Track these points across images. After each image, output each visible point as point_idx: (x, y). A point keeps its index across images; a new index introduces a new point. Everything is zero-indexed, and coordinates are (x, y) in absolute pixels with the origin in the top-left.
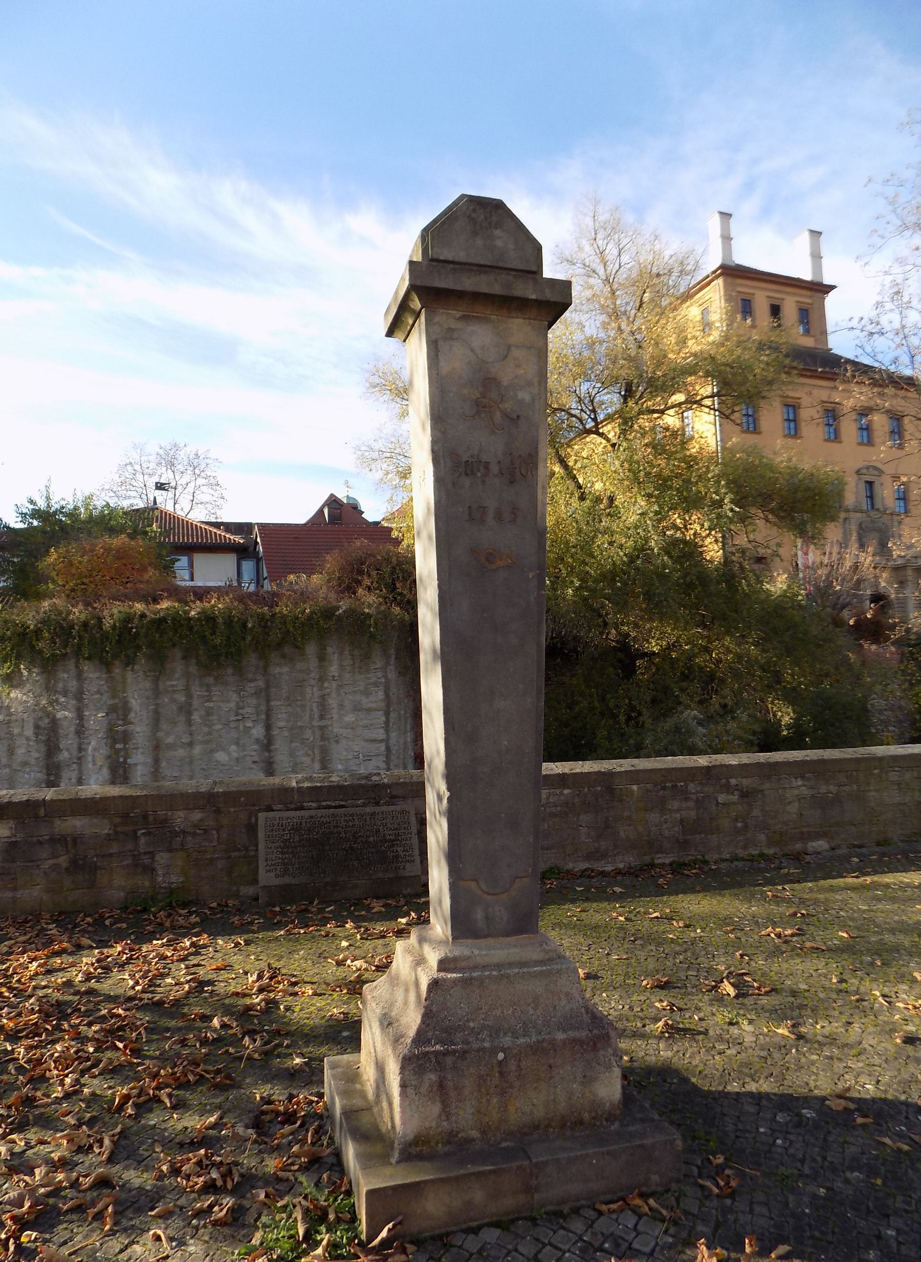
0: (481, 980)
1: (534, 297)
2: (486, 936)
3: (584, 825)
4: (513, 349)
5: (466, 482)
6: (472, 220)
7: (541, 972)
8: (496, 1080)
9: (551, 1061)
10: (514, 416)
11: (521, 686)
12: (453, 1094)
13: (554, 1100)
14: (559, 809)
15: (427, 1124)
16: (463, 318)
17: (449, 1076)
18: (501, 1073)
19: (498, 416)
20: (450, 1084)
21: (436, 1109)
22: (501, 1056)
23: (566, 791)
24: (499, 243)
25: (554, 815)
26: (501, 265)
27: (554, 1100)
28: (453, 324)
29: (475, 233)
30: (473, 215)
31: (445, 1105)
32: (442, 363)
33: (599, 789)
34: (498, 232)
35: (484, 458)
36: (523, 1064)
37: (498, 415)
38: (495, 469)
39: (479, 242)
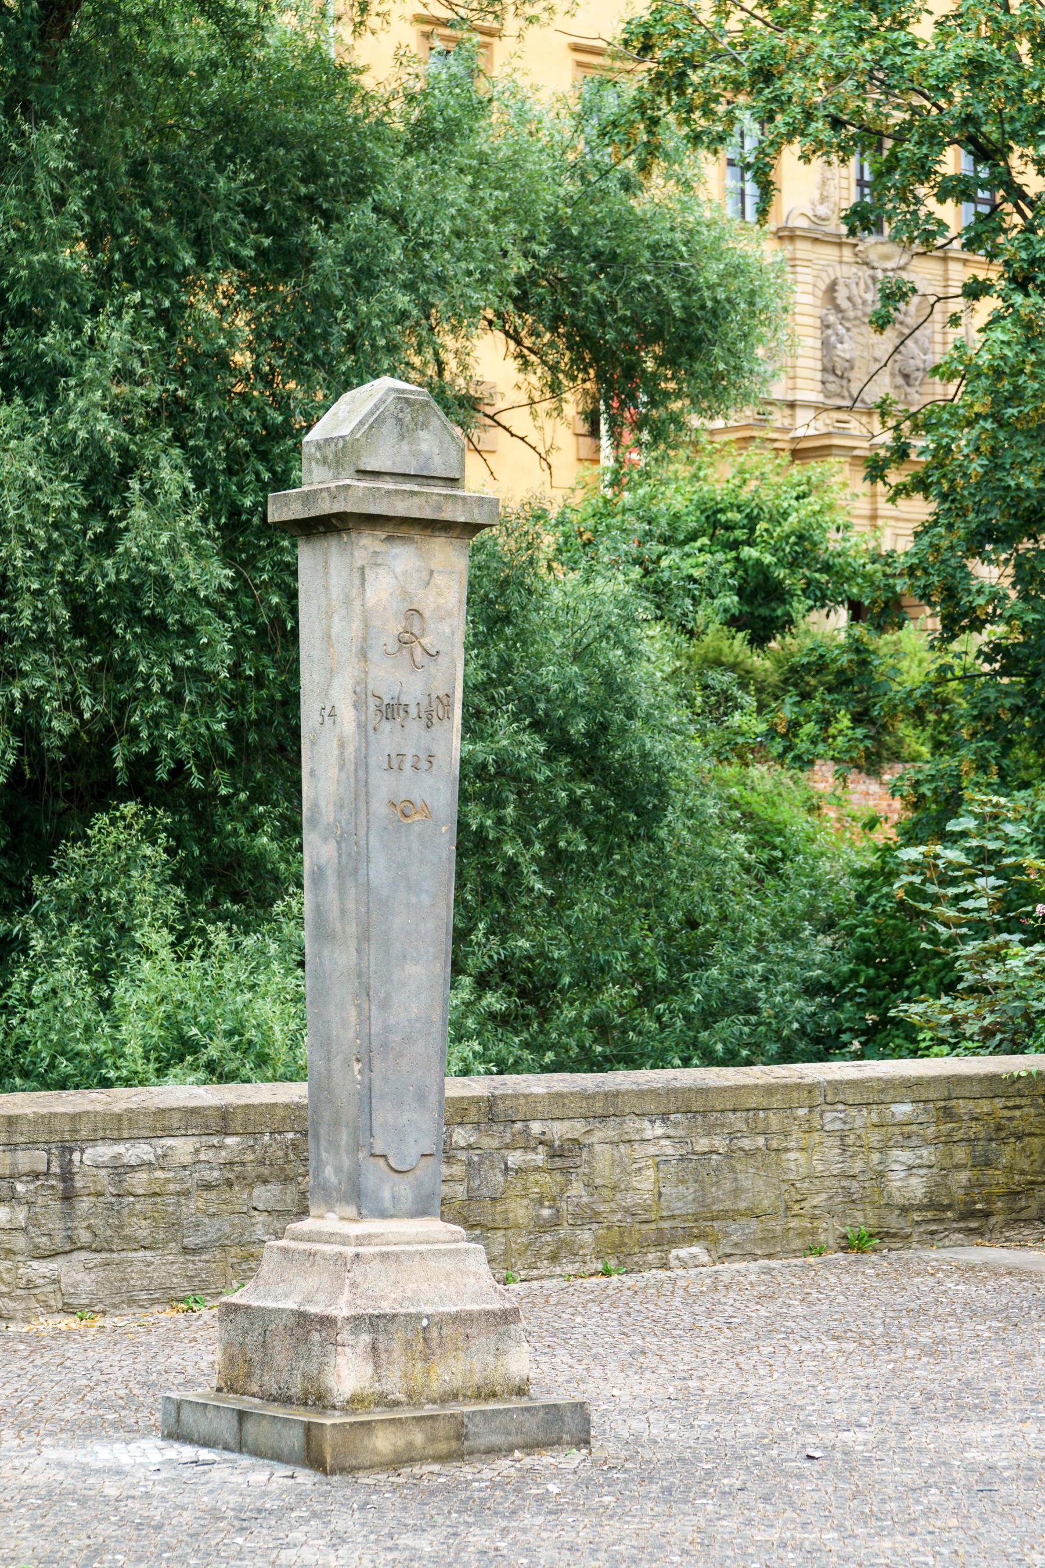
0: (397, 1255)
1: (462, 519)
2: (392, 1216)
3: (261, 1207)
4: (435, 575)
5: (386, 726)
6: (400, 421)
7: (451, 1251)
8: (420, 1346)
9: (469, 1331)
10: (433, 652)
11: (431, 950)
12: (384, 1356)
13: (470, 1371)
14: (216, 1174)
15: (362, 1384)
16: (389, 538)
17: (381, 1338)
18: (424, 1339)
19: (418, 651)
20: (381, 1347)
21: (369, 1369)
22: (425, 1322)
23: (230, 1141)
24: (424, 447)
25: (208, 1187)
26: (425, 473)
27: (470, 1371)
28: (379, 547)
29: (402, 437)
30: (401, 415)
31: (377, 1366)
32: (368, 594)
33: (291, 1136)
34: (422, 434)
35: (404, 700)
36: (444, 1332)
37: (418, 651)
38: (413, 710)
39: (405, 447)
